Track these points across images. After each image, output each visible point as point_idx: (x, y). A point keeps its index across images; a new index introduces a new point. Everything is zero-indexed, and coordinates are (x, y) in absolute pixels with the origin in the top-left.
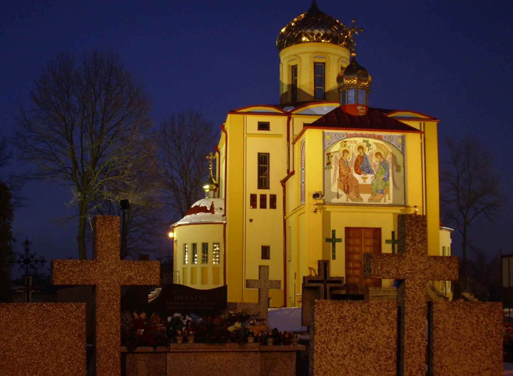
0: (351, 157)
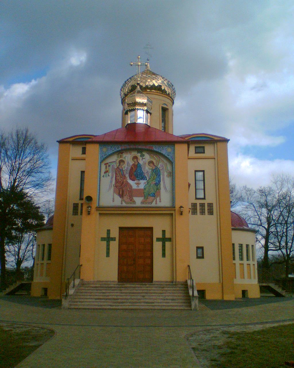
0: (126, 166)
